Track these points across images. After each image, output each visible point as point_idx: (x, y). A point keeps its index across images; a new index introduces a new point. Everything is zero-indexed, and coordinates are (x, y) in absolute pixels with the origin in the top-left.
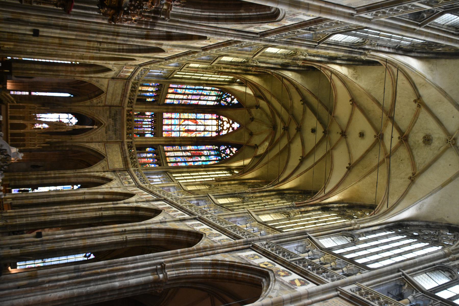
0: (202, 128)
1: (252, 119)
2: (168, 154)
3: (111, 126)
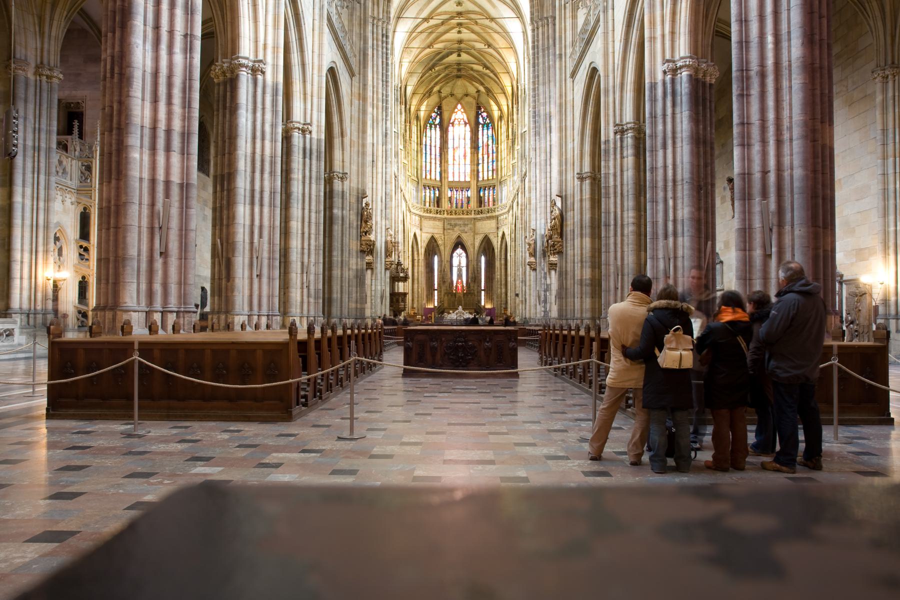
0: (462, 142)
1: (452, 95)
2: (486, 178)
3: (462, 228)
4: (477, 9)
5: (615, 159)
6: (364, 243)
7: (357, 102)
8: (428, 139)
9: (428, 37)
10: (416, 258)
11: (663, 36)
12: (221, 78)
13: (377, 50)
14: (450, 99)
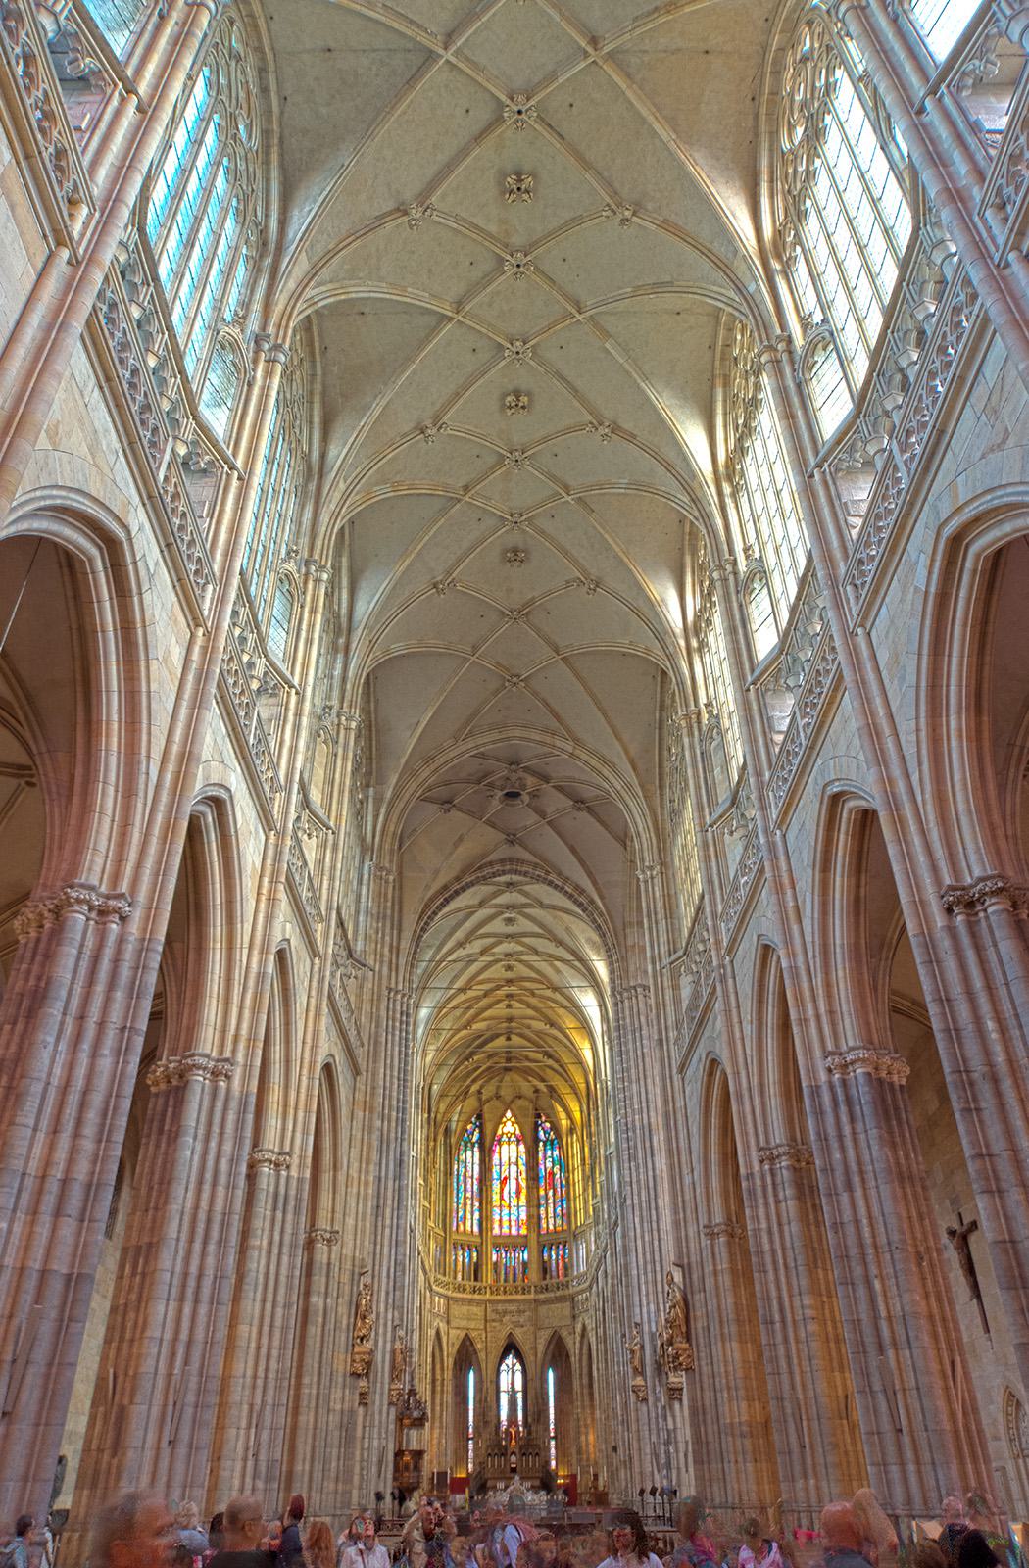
0: (514, 1168)
1: (498, 1097)
4: (534, 975)
5: (767, 1204)
6: (357, 1357)
7: (361, 1114)
8: (462, 1166)
9: (464, 1014)
10: (438, 1377)
11: (818, 1017)
12: (163, 1086)
13: (393, 1035)
14: (495, 1103)
